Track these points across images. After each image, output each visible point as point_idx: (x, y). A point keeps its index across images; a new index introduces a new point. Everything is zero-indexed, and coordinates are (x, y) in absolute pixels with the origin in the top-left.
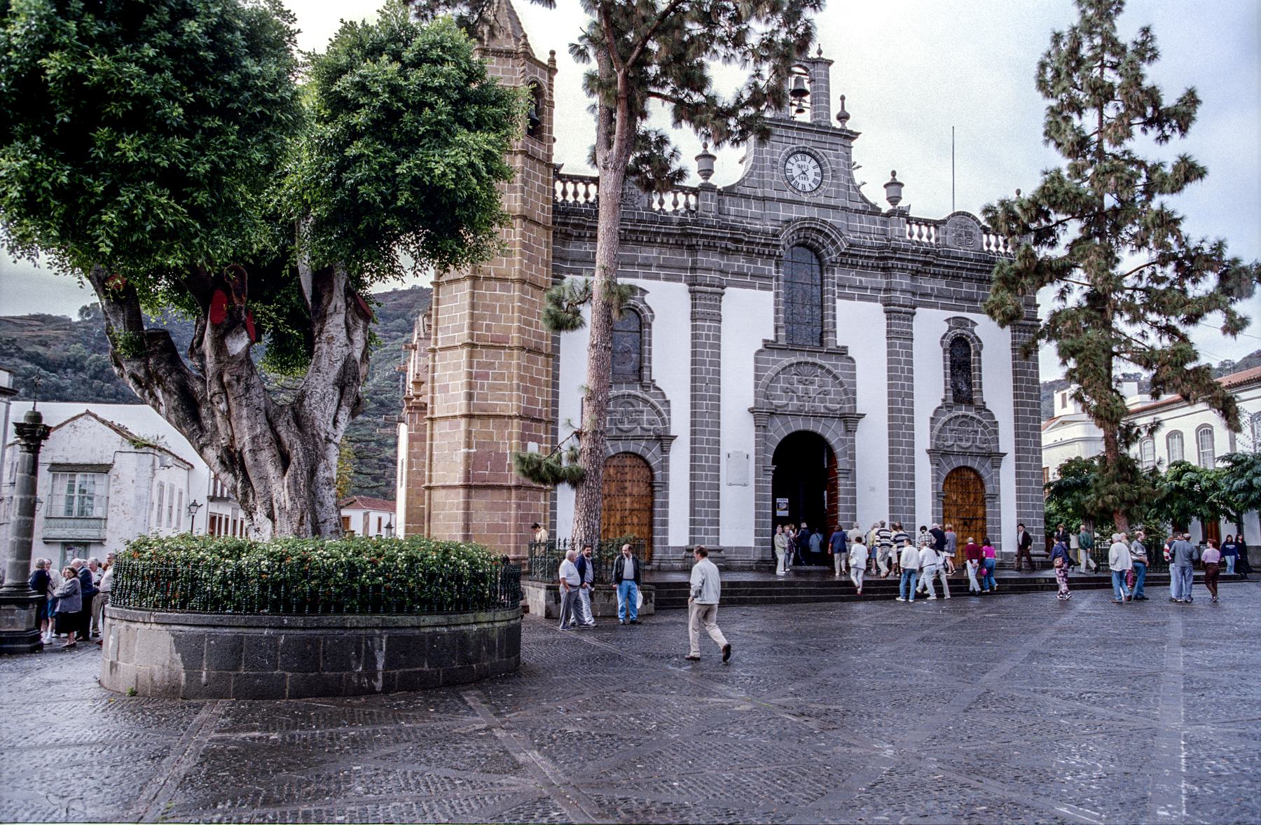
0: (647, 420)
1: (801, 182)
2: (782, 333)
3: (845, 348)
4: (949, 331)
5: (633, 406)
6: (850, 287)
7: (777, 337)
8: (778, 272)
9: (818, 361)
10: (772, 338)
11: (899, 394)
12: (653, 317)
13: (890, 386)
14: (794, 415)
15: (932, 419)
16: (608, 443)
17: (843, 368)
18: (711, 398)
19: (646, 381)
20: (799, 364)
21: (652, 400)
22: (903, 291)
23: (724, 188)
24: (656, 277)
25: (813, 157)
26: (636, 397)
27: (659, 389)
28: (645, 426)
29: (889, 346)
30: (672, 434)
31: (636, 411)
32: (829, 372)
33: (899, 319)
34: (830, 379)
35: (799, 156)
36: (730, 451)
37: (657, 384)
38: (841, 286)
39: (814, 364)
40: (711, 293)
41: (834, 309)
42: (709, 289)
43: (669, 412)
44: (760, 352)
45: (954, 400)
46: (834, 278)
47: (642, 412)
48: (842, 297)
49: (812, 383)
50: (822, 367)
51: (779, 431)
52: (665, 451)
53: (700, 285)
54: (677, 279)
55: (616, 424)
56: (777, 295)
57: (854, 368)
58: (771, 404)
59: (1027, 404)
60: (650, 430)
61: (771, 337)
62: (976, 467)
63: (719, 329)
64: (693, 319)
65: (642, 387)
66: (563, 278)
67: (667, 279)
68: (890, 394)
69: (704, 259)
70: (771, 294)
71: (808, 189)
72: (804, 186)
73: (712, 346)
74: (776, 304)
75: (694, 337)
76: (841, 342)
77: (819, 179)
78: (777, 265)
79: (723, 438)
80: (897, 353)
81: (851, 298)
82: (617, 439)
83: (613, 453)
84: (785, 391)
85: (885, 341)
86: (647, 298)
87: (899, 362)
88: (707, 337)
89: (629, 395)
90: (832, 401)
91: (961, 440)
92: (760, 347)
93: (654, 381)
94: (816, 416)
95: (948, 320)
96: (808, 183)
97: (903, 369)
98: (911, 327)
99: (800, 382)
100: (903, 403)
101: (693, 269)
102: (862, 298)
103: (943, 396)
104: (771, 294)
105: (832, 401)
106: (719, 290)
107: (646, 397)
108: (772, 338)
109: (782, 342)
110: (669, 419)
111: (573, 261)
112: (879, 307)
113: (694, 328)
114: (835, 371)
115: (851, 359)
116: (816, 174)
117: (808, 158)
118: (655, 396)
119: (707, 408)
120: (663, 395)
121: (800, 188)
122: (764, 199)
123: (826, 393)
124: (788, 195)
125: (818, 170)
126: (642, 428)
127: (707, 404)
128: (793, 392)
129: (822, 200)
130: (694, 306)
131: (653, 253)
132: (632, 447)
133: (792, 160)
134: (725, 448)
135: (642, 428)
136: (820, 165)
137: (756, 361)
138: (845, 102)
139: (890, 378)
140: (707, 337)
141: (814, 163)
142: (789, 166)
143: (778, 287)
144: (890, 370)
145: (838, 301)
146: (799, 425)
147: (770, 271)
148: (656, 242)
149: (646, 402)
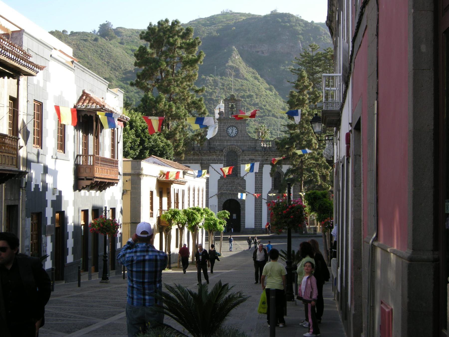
6: (244, 161)
11: (258, 188)
13: (255, 186)
17: (242, 182)
24: (192, 163)
25: (235, 127)
36: (211, 205)
38: (242, 161)
41: (240, 167)
42: (205, 165)
44: (219, 180)
45: (274, 189)
49: (234, 187)
51: (224, 199)
57: (245, 182)
59: (297, 189)
67: (195, 163)
68: (255, 188)
69: (204, 158)
71: (233, 136)
72: (232, 135)
78: (224, 157)
87: (258, 180)
96: (233, 135)
98: (262, 170)
100: (259, 191)
101: (202, 160)
103: (271, 188)
115: (245, 180)
116: (236, 131)
117: (234, 127)
122: (220, 140)
124: (227, 138)
125: (237, 130)
129: (237, 138)
133: (229, 128)
142: (228, 130)
143: (224, 163)
144: (255, 182)
147: (222, 159)
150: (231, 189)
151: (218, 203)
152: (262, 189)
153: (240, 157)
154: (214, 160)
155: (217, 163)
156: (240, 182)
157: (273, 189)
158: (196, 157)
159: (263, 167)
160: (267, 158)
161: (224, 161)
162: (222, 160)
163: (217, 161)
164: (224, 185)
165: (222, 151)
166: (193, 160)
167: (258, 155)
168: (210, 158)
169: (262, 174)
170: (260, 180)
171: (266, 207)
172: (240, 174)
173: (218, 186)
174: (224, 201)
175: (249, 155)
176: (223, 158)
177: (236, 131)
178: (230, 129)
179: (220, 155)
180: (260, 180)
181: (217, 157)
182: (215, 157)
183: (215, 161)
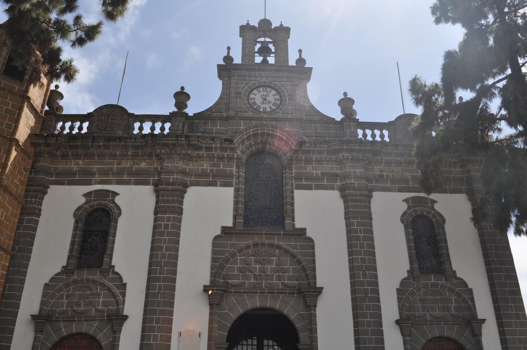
0: (103, 302)
1: (262, 106)
2: (240, 220)
3: (304, 230)
4: (409, 208)
5: (91, 290)
6: (307, 179)
7: (234, 223)
8: (239, 172)
9: (276, 242)
10: (231, 225)
12: (120, 214)
14: (252, 291)
15: (398, 291)
16: (62, 325)
18: (165, 280)
19: (105, 267)
20: (256, 245)
21: (110, 284)
22: (356, 178)
23: (194, 114)
26: (94, 281)
27: (117, 274)
28: (100, 307)
29: (348, 225)
30: (125, 313)
31: (92, 295)
32: (287, 252)
33: (356, 201)
34: (288, 259)
35: (261, 89)
37: (116, 269)
39: (271, 245)
40: (172, 190)
41: (293, 198)
43: (124, 295)
44: (216, 238)
46: (292, 174)
47: (99, 295)
48: (299, 187)
49: (270, 262)
50: (279, 247)
52: (116, 331)
53: (163, 185)
54: (146, 183)
55: (72, 307)
56: (237, 190)
57: (313, 247)
58: (228, 283)
60: (103, 312)
61: (229, 223)
62: (453, 336)
63: (180, 220)
64: (156, 213)
65: (101, 272)
66: (49, 187)
67: (137, 183)
69: (168, 164)
70: (230, 191)
73: (169, 234)
74: (236, 196)
75: (155, 227)
76: (299, 224)
77: (278, 102)
78: (238, 167)
79: (176, 317)
80: (356, 231)
81: (308, 188)
82: (71, 320)
83: (65, 334)
84: (240, 270)
85: (344, 222)
86: (117, 200)
87: (358, 239)
88: (166, 226)
89: (88, 280)
90: (289, 278)
91: (433, 309)
92: (218, 232)
93: (114, 267)
94: (272, 291)
95: (406, 200)
97: (362, 246)
99: (256, 262)
100: (365, 276)
102: (318, 187)
103: (408, 267)
104: (230, 191)
105: (289, 278)
106: (180, 187)
107: (105, 281)
108: (231, 225)
109: (240, 227)
110: (124, 301)
111: (58, 174)
112: (336, 194)
113: (156, 220)
114: (292, 250)
115: (311, 240)
116: (275, 100)
118: (111, 280)
119: (160, 289)
120: (121, 278)
121: (261, 110)
123: (284, 271)
125: (278, 97)
126: (96, 309)
127: (160, 286)
128: (250, 271)
130: (157, 202)
131: (127, 164)
132: (84, 328)
133: (255, 92)
134: (176, 328)
135: (96, 310)
136: (279, 93)
137: (214, 245)
138: (302, 54)
139: (350, 254)
140: (166, 226)
141: (274, 92)
142: (252, 96)
145: (295, 190)
146: (256, 302)
148: (127, 155)
149: (103, 285)
150: (263, 271)
151: (211, 321)
152: (375, 269)
153: (291, 168)
154: (204, 174)
155: (214, 184)
156: (295, 247)
157: (417, 272)
158: (143, 165)
159: (371, 197)
160: (381, 171)
161: (238, 177)
162: (231, 176)
163: (214, 176)
164: (234, 255)
165: (231, 141)
166: (131, 173)
167: (353, 160)
168: (191, 166)
169: (371, 219)
170: (365, 238)
171: (399, 339)
172: (293, 219)
173: (214, 260)
174: (234, 317)
175: (319, 161)
176: (234, 169)
177: (275, 100)
178: (259, 95)
179: (221, 158)
180: (365, 238)
181: (214, 165)
182: (206, 166)
183: (208, 176)
